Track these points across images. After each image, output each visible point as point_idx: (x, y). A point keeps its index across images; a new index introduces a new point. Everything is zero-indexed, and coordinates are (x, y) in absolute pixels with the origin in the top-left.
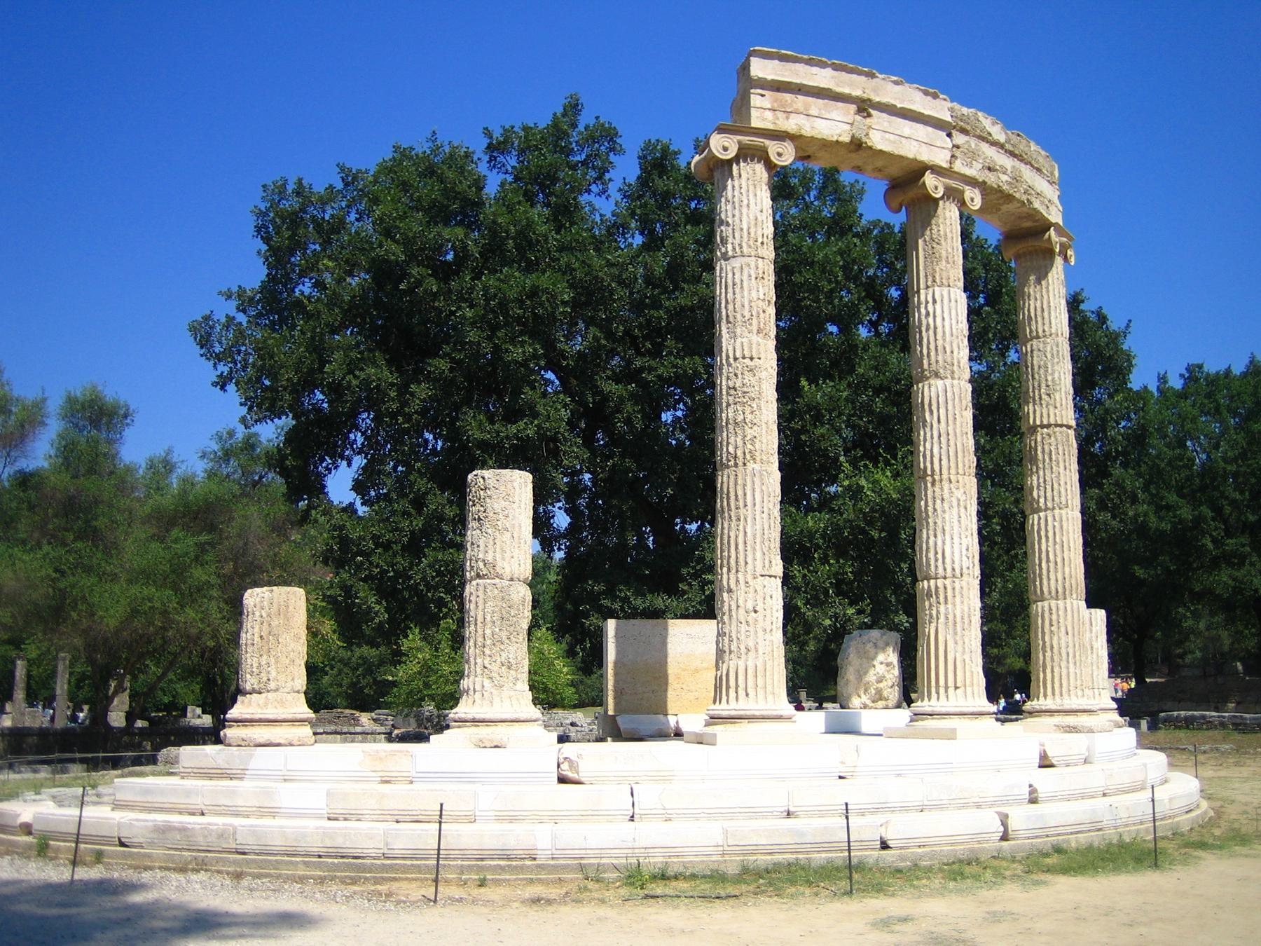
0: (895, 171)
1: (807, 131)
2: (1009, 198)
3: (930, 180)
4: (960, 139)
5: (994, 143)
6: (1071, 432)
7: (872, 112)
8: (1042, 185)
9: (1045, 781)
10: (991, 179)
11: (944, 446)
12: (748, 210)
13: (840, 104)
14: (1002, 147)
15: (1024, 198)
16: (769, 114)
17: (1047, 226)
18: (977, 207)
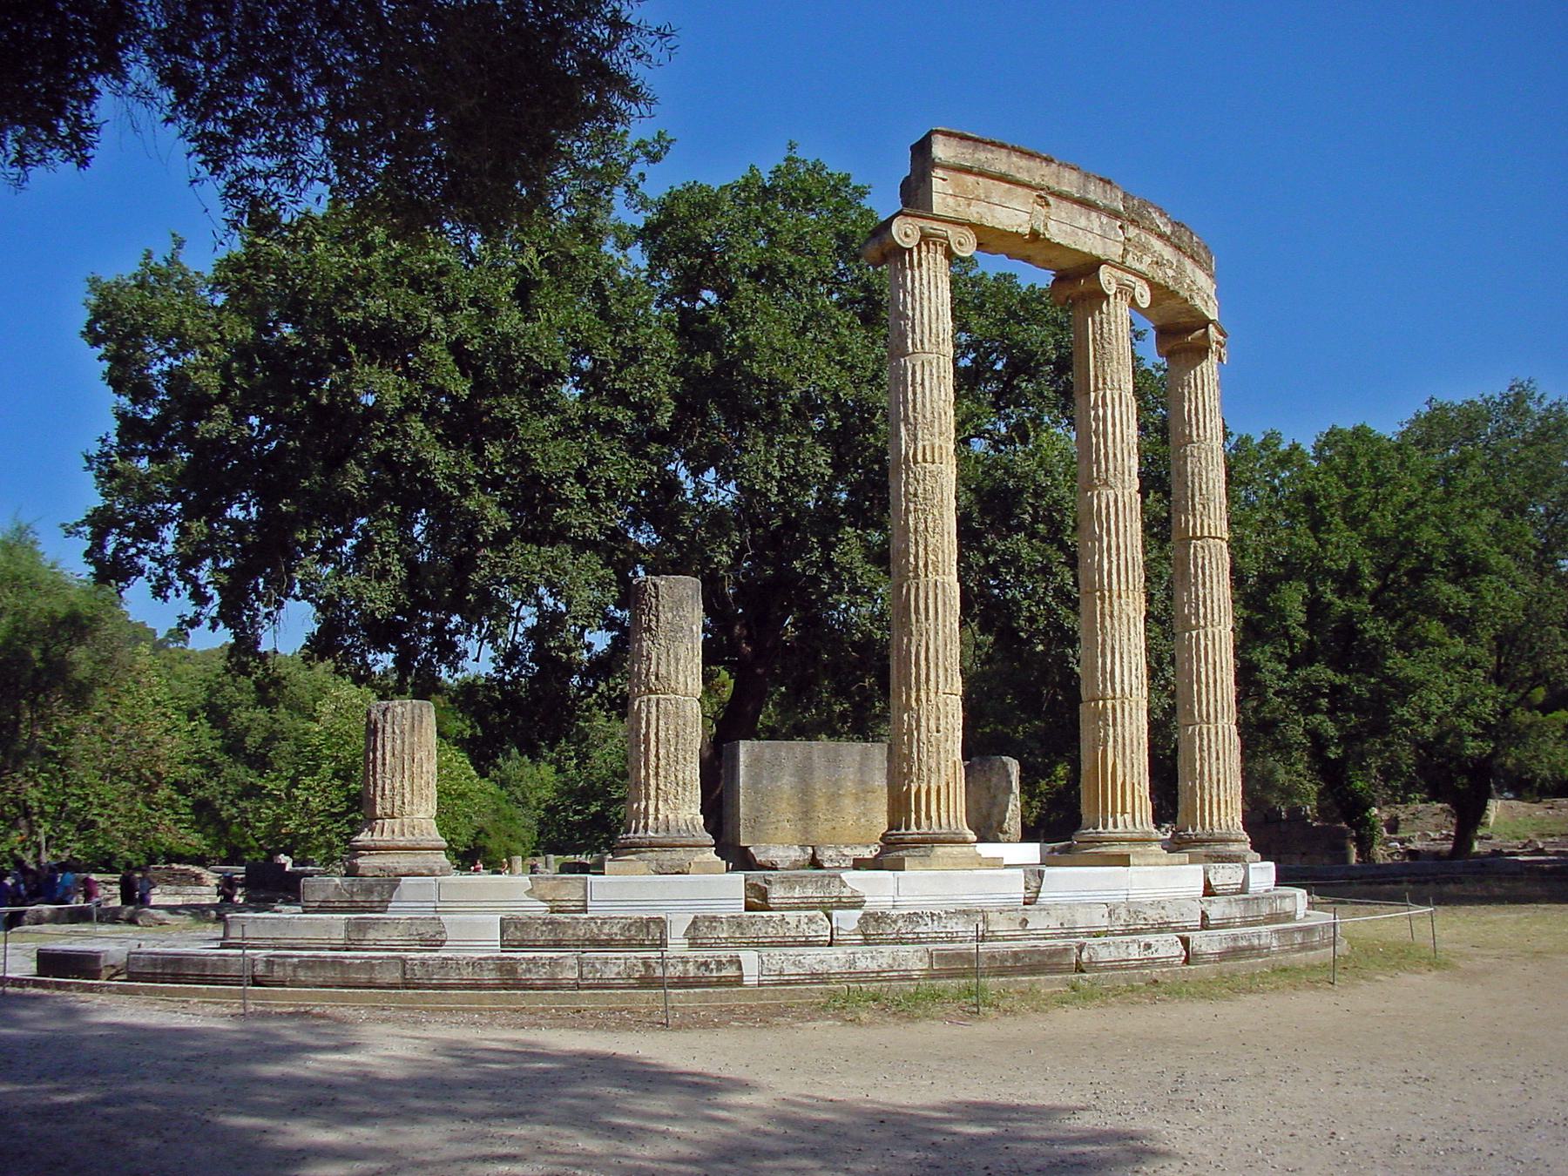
0: (1066, 263)
1: (989, 222)
2: (1174, 294)
3: (1105, 274)
4: (1132, 232)
5: (1161, 236)
6: (1225, 545)
7: (1051, 199)
8: (1202, 279)
9: (1217, 909)
10: (1158, 276)
11: (1114, 559)
12: (930, 298)
13: (1020, 189)
14: (1168, 239)
15: (1187, 294)
16: (950, 200)
17: (1206, 323)
18: (1146, 306)
